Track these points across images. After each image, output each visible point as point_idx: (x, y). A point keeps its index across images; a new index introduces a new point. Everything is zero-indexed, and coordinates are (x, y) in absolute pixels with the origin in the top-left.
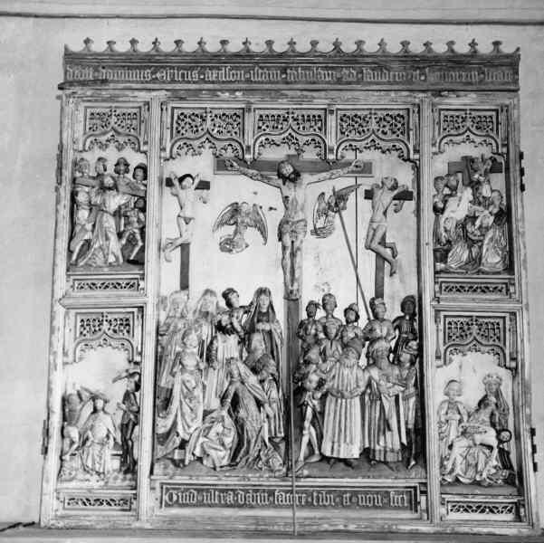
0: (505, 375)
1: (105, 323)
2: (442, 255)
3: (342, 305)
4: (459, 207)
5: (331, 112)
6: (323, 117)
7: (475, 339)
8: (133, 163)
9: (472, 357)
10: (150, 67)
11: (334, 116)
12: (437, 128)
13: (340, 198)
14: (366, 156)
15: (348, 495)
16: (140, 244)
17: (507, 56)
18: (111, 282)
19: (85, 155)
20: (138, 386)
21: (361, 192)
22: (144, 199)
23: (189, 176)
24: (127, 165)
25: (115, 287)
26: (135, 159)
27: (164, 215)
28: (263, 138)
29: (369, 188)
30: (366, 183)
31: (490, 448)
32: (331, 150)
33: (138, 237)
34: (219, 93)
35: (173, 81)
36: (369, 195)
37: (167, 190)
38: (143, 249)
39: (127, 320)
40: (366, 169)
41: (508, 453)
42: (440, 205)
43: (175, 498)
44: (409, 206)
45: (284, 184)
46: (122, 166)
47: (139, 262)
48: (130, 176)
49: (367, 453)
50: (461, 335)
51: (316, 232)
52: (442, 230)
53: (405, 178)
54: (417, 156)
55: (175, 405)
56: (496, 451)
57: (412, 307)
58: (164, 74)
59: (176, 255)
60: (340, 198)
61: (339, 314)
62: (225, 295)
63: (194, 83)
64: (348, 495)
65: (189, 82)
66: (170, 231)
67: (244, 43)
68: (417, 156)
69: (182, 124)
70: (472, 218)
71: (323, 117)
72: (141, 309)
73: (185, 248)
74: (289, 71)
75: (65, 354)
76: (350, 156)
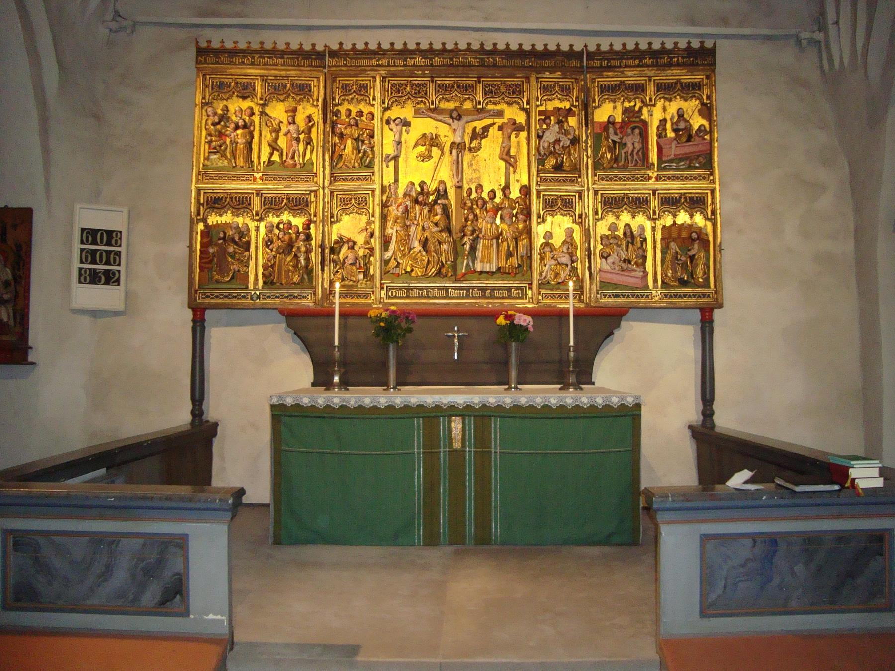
0: (576, 227)
1: (353, 200)
2: (541, 161)
3: (487, 189)
4: (550, 137)
5: (479, 82)
6: (475, 85)
7: (559, 207)
8: (366, 111)
9: (559, 218)
10: (375, 58)
11: (481, 85)
12: (539, 91)
13: (486, 129)
14: (498, 107)
15: (489, 291)
16: (371, 156)
17: (578, 52)
18: (355, 177)
19: (339, 108)
20: (372, 235)
21: (496, 127)
22: (373, 131)
23: (399, 118)
24: (363, 112)
25: (358, 180)
26: (366, 110)
27: (386, 141)
28: (441, 97)
29: (500, 125)
30: (499, 121)
31: (567, 266)
32: (479, 103)
33: (370, 152)
34: (416, 72)
35: (389, 65)
36: (500, 128)
37: (386, 127)
38: (374, 157)
39: (366, 198)
40: (500, 114)
41: (577, 269)
42: (541, 134)
43: (394, 294)
44: (523, 134)
45: (453, 122)
46: (360, 114)
47: (370, 166)
48: (364, 118)
49: (499, 269)
50: (551, 206)
51: (470, 149)
52: (542, 147)
53: (521, 118)
54: (528, 107)
55: (392, 246)
56: (569, 266)
57: (526, 191)
58: (384, 62)
59: (392, 163)
60: (486, 129)
61: (485, 195)
62: (419, 185)
63: (401, 66)
64: (489, 291)
65: (397, 66)
66: (389, 149)
67: (429, 44)
68: (528, 107)
69: (394, 89)
70: (558, 141)
71: (475, 85)
72: (373, 191)
73: (396, 158)
74: (454, 59)
75: (332, 216)
76: (490, 107)
